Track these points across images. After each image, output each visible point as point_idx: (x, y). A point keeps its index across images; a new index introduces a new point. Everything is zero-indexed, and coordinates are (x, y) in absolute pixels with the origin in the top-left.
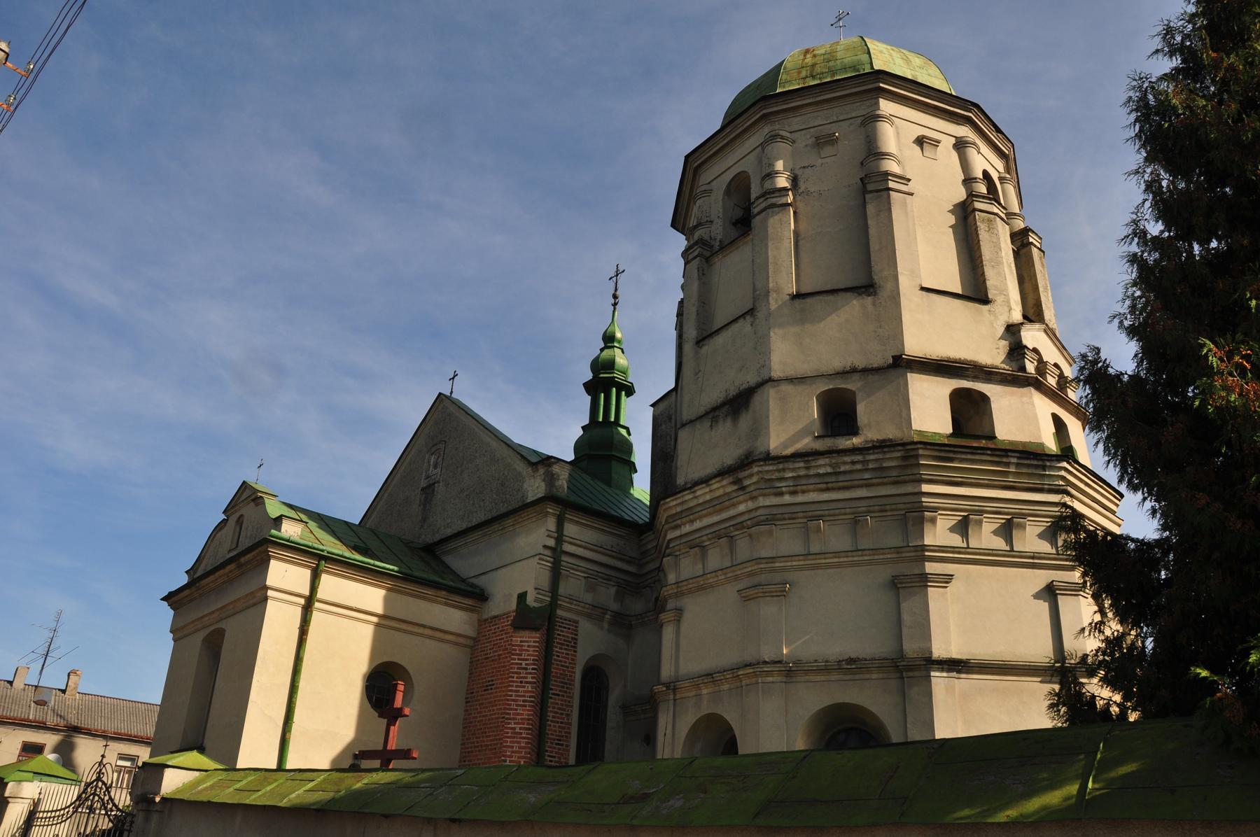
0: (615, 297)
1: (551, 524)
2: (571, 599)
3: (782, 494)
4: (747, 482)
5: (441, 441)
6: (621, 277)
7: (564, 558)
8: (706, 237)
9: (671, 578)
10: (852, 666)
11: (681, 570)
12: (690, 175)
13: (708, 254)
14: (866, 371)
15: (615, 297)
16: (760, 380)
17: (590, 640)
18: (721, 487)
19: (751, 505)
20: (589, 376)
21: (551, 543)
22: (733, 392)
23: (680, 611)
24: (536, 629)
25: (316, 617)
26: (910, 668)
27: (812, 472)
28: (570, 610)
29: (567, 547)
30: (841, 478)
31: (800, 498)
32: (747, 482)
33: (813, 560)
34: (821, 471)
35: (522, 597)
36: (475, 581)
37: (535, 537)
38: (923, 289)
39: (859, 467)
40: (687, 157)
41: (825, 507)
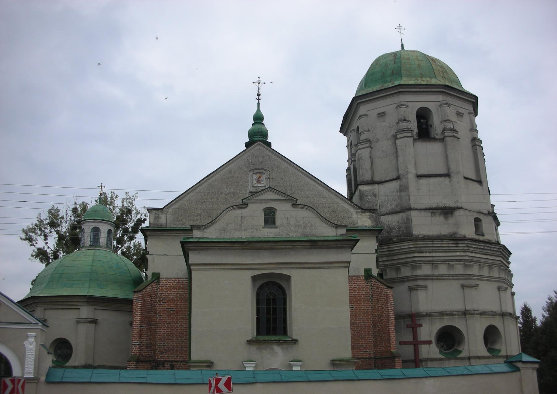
0: (259, 95)
4: (459, 245)
10: (493, 314)
15: (259, 95)
18: (451, 244)
19: (463, 254)
26: (505, 316)
30: (484, 251)
32: (459, 245)
33: (482, 278)
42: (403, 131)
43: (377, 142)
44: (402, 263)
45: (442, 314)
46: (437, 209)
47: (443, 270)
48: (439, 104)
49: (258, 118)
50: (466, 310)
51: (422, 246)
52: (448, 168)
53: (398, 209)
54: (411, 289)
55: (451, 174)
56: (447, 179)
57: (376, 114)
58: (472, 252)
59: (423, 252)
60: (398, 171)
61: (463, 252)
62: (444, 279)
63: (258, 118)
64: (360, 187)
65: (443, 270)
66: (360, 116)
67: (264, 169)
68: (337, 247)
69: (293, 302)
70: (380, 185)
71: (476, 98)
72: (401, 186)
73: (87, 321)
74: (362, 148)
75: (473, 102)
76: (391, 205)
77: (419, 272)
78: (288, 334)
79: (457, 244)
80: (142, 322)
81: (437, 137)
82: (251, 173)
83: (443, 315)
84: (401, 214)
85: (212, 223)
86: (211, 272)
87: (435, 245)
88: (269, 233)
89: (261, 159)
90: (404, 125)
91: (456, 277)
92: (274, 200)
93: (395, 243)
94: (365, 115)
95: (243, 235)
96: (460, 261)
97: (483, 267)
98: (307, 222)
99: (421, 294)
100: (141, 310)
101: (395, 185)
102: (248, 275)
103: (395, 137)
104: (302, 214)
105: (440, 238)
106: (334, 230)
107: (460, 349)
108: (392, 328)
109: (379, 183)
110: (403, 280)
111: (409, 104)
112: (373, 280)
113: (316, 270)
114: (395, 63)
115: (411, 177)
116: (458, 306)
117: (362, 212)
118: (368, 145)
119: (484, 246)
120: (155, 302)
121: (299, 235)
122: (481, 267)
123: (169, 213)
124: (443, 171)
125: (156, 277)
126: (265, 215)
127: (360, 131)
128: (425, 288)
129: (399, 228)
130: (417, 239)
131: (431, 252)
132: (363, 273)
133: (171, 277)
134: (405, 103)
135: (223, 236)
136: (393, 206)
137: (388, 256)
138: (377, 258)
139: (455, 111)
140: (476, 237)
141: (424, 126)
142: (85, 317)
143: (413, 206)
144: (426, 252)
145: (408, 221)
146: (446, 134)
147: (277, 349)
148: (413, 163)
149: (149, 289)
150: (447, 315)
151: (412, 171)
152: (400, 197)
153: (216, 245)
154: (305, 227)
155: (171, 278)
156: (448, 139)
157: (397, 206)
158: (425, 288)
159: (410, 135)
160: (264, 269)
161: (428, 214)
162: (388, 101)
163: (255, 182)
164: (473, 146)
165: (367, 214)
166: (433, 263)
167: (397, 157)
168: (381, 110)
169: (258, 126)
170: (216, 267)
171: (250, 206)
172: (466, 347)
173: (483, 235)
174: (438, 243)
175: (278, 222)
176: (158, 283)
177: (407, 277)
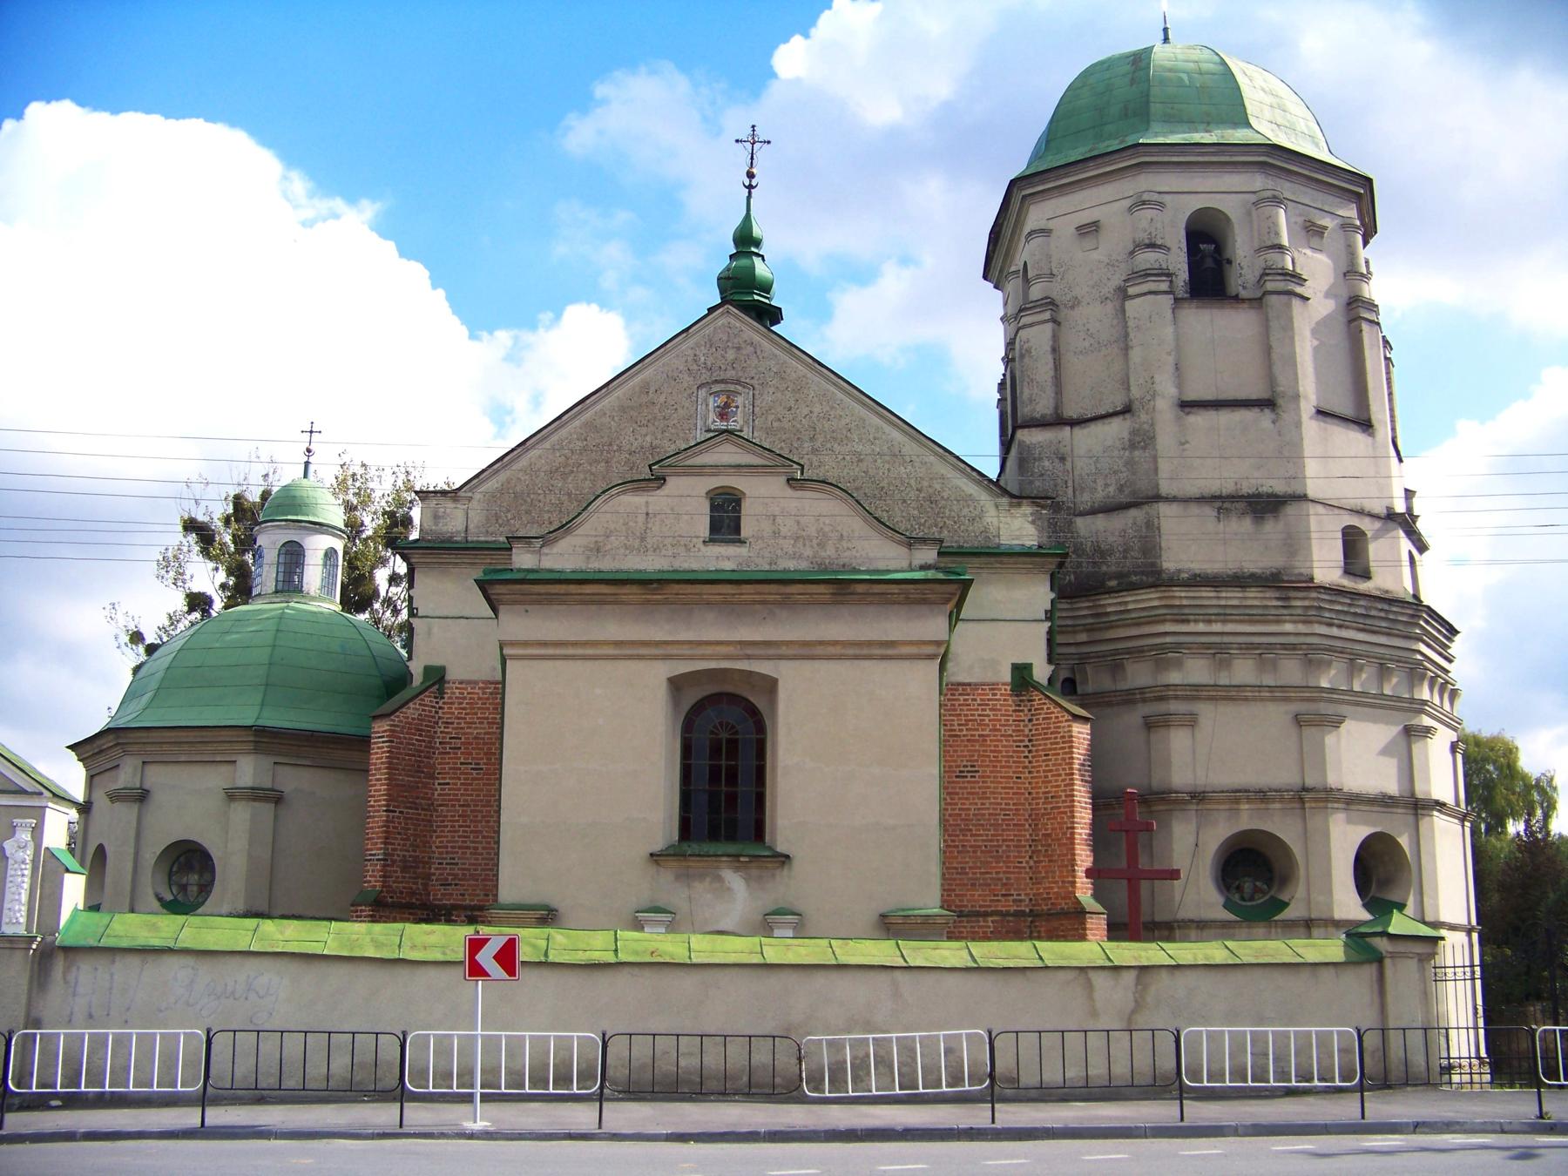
0: (751, 175)
6: (762, 153)
10: (1384, 802)
15: (751, 175)
16: (1290, 491)
19: (1302, 628)
30: (1368, 621)
34: (1359, 611)
42: (1146, 274)
43: (1072, 307)
44: (1129, 651)
45: (1237, 795)
46: (1233, 498)
47: (1243, 671)
48: (1253, 198)
49: (746, 241)
50: (1305, 789)
51: (1185, 602)
52: (1272, 381)
53: (1123, 499)
54: (1150, 725)
55: (1280, 401)
56: (1264, 418)
57: (1072, 230)
58: (1330, 625)
59: (1188, 621)
60: (1128, 389)
61: (1304, 622)
62: (1246, 699)
63: (746, 241)
64: (1022, 435)
65: (1243, 671)
66: (1030, 234)
67: (738, 382)
68: (909, 601)
69: (781, 752)
70: (1077, 430)
71: (1368, 182)
72: (1134, 432)
73: (256, 795)
74: (1031, 325)
75: (1358, 195)
76: (1107, 485)
77: (1174, 677)
78: (767, 838)
79: (1287, 599)
80: (391, 798)
81: (1244, 294)
82: (703, 393)
83: (1237, 801)
84: (1133, 512)
85: (565, 528)
86: (558, 663)
87: (1223, 602)
88: (723, 558)
89: (731, 355)
90: (1148, 259)
91: (1281, 693)
92: (739, 466)
93: (1110, 591)
94: (1042, 231)
95: (651, 564)
96: (1294, 647)
97: (1361, 668)
98: (827, 529)
99: (1178, 740)
100: (391, 767)
101: (1116, 430)
102: (657, 674)
103: (1123, 294)
104: (819, 509)
105: (1240, 581)
106: (904, 550)
107: (1284, 897)
108: (1082, 831)
109: (1074, 423)
110: (1130, 698)
111: (1167, 199)
112: (1036, 696)
113: (848, 663)
114: (1133, 82)
115: (1164, 406)
116: (1283, 775)
117: (1011, 505)
118: (1047, 315)
119: (1366, 608)
120: (430, 745)
121: (804, 565)
122: (1353, 669)
123: (474, 504)
124: (1256, 391)
125: (436, 677)
126: (713, 508)
127: (1030, 275)
128: (1191, 721)
129: (1125, 551)
130: (1173, 582)
131: (1210, 622)
132: (1008, 679)
133: (475, 677)
134: (1155, 197)
135: (595, 565)
136: (1111, 489)
137: (1090, 629)
138: (1050, 632)
139: (1300, 220)
140: (1347, 583)
141: (1209, 263)
142: (250, 784)
143: (1165, 488)
144: (1196, 621)
145: (1152, 527)
146: (1270, 286)
147: (734, 879)
148: (1170, 368)
149: (412, 711)
150: (1249, 800)
151: (1167, 390)
152: (1130, 463)
153: (573, 588)
154: (821, 545)
155: (476, 682)
156: (1273, 299)
157: (1121, 489)
158: (1191, 721)
159: (1164, 286)
160: (703, 658)
161: (1209, 511)
162: (1107, 191)
163: (712, 416)
164: (1350, 322)
165: (1027, 509)
166: (1219, 652)
167: (1126, 349)
168: (1085, 217)
170: (570, 651)
171: (674, 484)
172: (1300, 892)
173: (1366, 575)
174: (1232, 597)
175: (746, 530)
176: (441, 693)
177: (1142, 690)
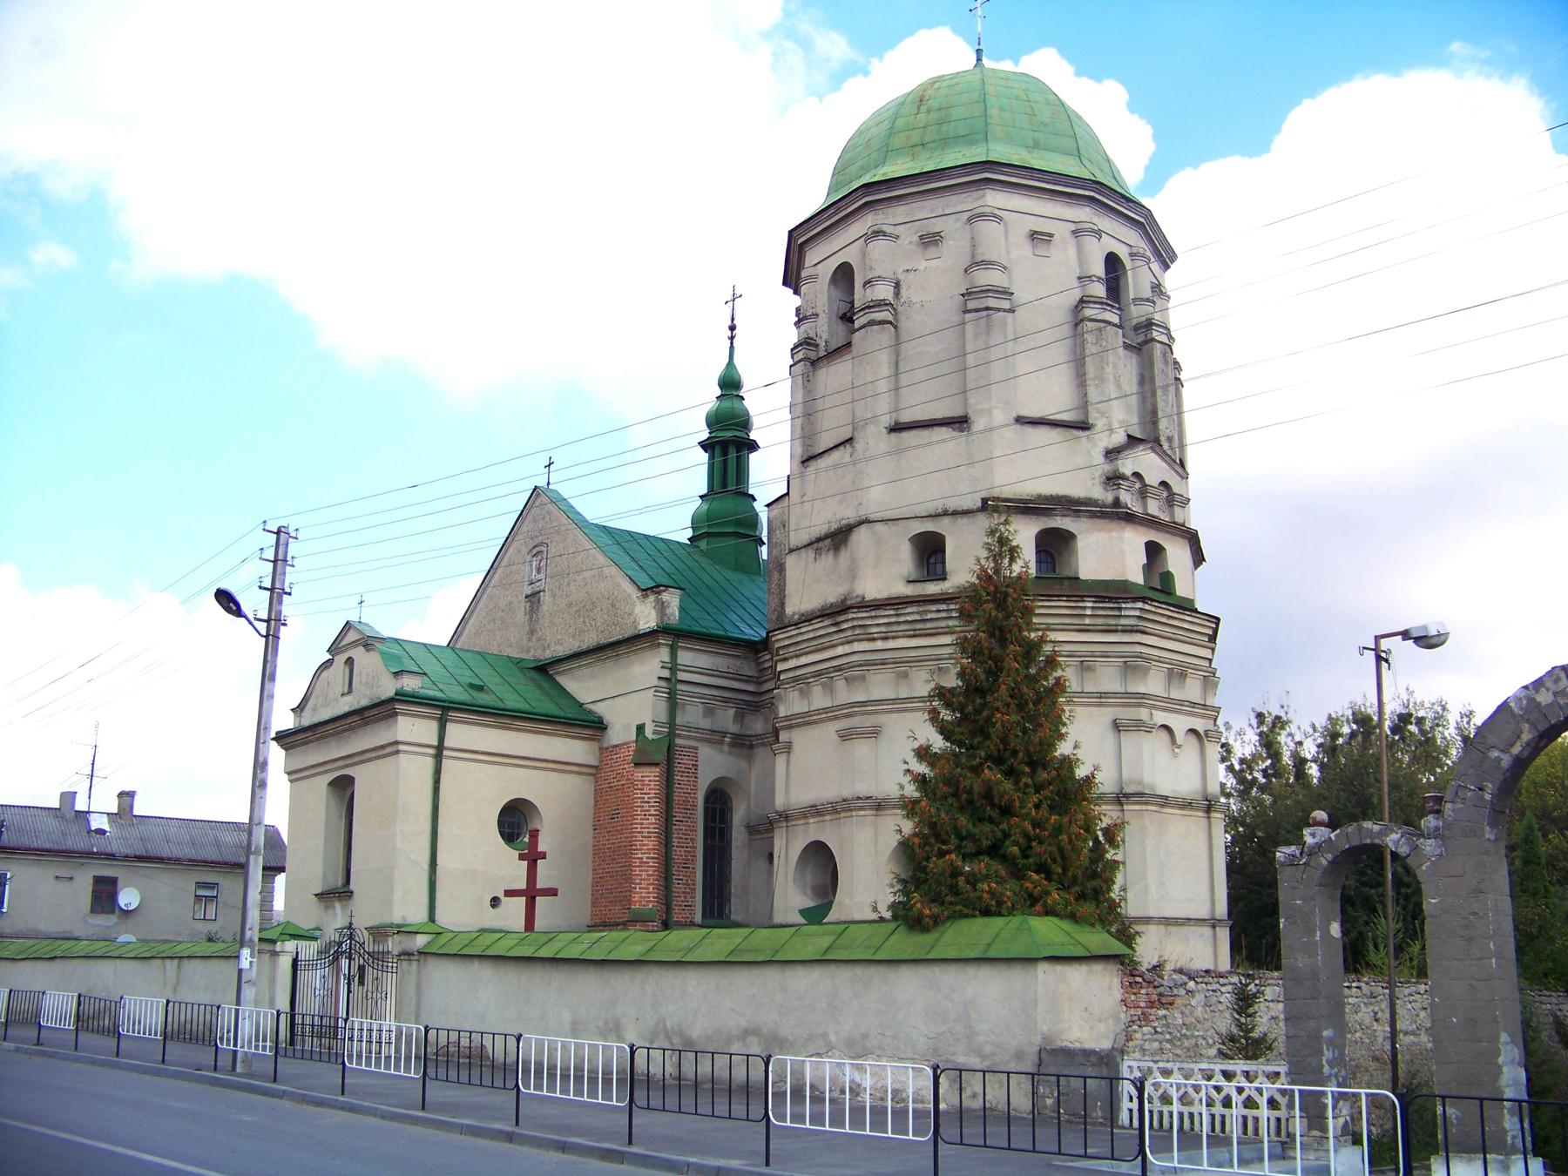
0: (732, 328)
1: (664, 654)
2: (689, 728)
3: (874, 639)
5: (542, 544)
7: (680, 687)
8: (812, 335)
9: (782, 712)
11: (790, 704)
12: (794, 259)
13: (813, 355)
14: (955, 513)
15: (732, 328)
17: (711, 764)
18: (822, 627)
20: (705, 435)
21: (666, 673)
22: (834, 526)
23: (788, 748)
24: (657, 764)
25: (446, 764)
27: (902, 619)
28: (689, 738)
29: (682, 676)
30: (929, 625)
31: (891, 644)
34: (909, 618)
35: (640, 729)
36: (592, 707)
37: (648, 668)
38: (1021, 420)
39: (943, 615)
40: (790, 232)
41: (912, 653)
49: (730, 384)
62: (816, 722)
63: (730, 384)
139: (915, 238)
161: (811, 553)
169: (727, 404)
